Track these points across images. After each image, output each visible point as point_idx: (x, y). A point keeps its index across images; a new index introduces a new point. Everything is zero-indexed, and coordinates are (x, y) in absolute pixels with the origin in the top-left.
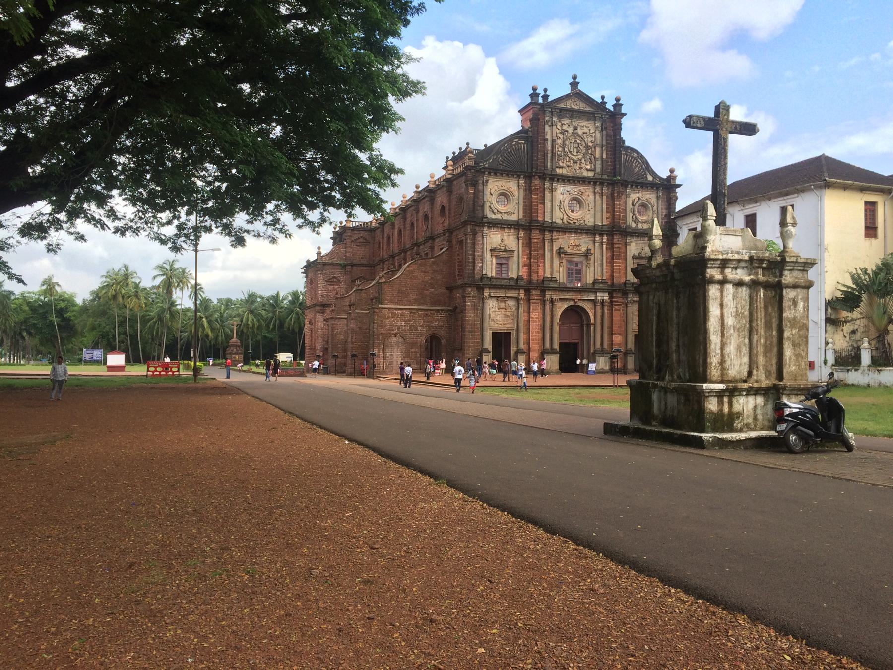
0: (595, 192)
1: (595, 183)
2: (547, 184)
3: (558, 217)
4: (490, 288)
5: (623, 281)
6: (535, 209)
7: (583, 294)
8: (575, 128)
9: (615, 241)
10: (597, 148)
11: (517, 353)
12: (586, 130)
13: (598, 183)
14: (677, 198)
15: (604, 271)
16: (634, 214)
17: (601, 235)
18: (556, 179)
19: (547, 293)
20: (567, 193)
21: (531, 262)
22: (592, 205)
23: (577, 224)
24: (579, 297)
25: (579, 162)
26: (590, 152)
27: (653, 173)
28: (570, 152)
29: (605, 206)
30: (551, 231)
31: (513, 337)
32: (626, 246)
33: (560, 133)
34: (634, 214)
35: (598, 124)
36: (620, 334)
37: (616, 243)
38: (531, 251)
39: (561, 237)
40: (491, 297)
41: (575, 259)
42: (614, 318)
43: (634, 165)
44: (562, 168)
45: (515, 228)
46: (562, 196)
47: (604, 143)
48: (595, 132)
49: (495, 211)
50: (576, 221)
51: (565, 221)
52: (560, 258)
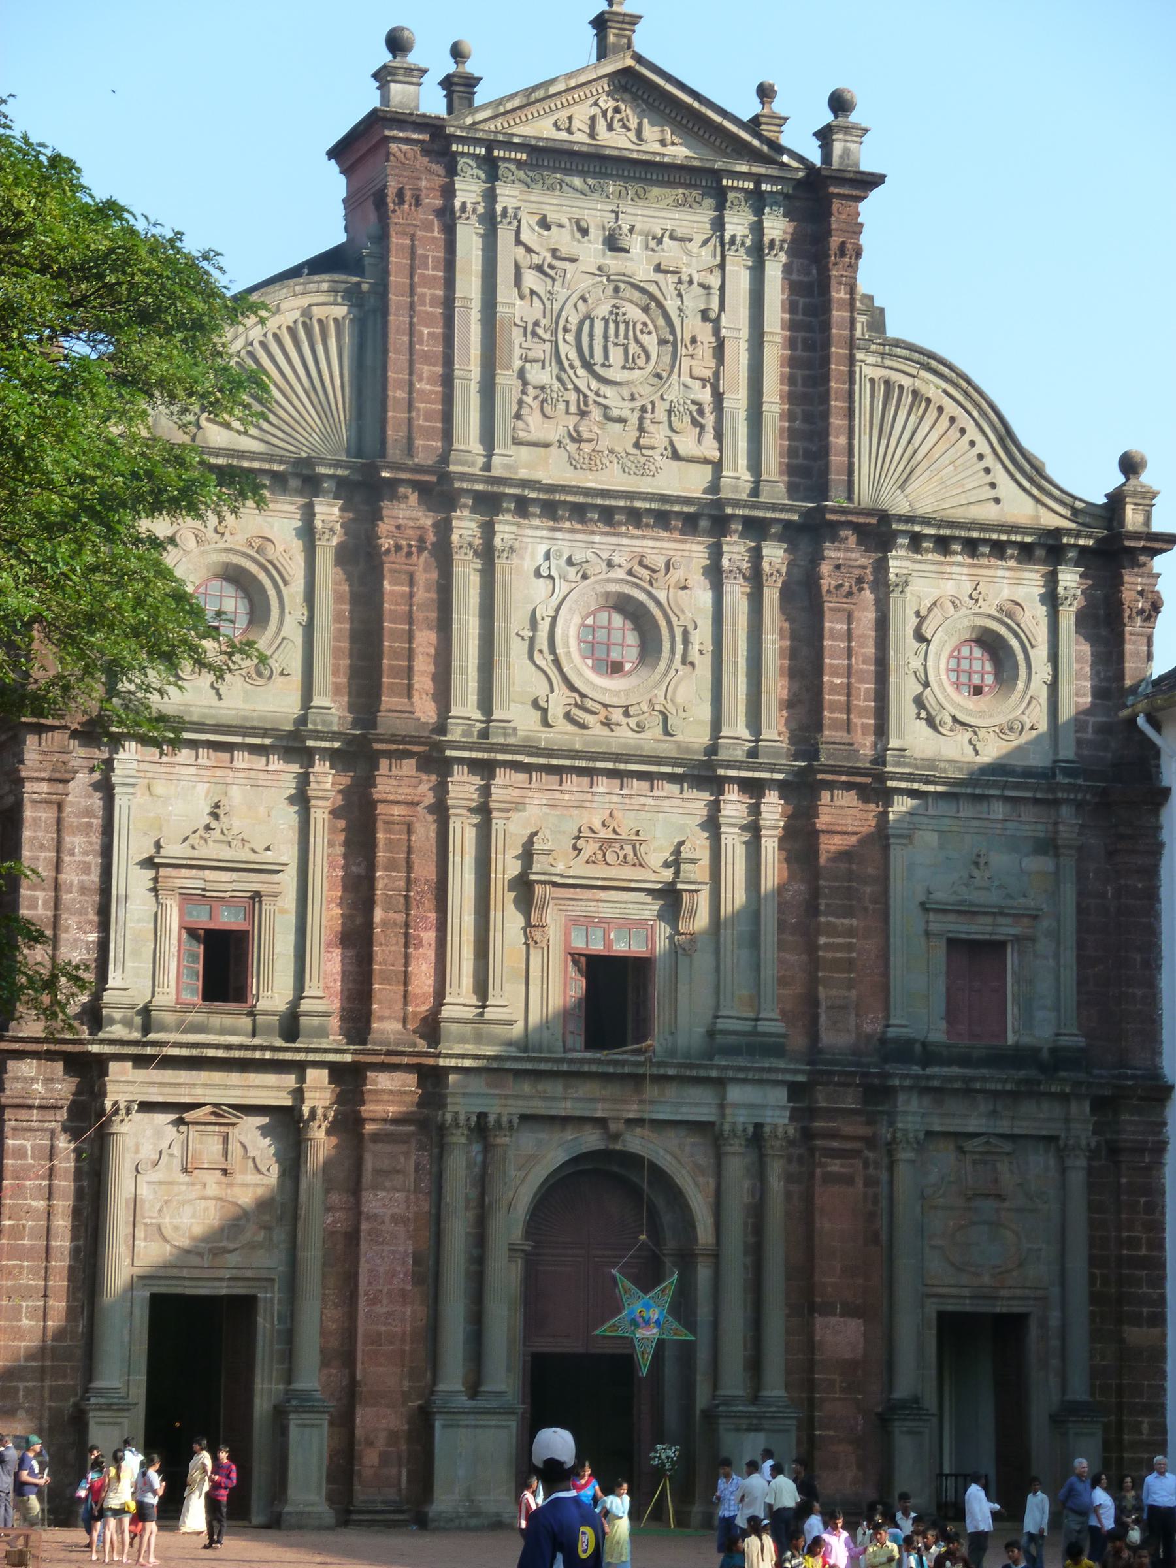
4: (141, 1061)
6: (395, 654)
7: (651, 1091)
9: (824, 819)
11: (280, 1414)
12: (670, 252)
14: (1156, 607)
15: (769, 972)
16: (926, 685)
17: (754, 788)
20: (572, 572)
21: (369, 924)
31: (266, 1324)
33: (539, 268)
35: (738, 224)
36: (850, 1311)
38: (371, 867)
40: (147, 1107)
41: (615, 906)
42: (823, 1224)
44: (547, 445)
46: (542, 585)
48: (722, 266)
50: (617, 715)
51: (556, 712)
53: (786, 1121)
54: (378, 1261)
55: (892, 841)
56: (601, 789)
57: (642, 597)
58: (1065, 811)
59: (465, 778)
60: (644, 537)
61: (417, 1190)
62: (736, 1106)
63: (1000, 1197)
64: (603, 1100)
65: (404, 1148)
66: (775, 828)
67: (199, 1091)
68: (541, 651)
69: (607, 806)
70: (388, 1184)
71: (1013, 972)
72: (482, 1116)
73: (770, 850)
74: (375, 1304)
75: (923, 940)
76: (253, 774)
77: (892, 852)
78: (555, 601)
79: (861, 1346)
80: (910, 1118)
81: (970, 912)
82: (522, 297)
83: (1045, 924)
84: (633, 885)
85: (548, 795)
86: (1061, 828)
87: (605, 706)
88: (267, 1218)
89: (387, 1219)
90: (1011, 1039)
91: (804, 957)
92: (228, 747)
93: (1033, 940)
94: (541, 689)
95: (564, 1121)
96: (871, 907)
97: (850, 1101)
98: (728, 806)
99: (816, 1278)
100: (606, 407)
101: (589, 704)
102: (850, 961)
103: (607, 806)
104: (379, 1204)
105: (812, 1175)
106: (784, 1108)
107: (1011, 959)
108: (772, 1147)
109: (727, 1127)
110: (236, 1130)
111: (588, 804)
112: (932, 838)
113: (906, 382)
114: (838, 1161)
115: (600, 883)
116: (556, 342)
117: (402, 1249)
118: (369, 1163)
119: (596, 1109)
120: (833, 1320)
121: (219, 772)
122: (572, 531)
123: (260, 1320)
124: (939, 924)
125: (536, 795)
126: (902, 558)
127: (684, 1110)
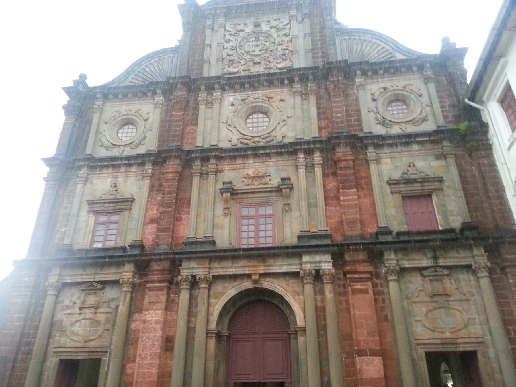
0: (294, 94)
1: (291, 81)
5: (371, 229)
7: (271, 261)
8: (257, 25)
12: (274, 23)
17: (309, 152)
18: (216, 86)
19: (185, 264)
23: (261, 144)
24: (262, 270)
27: (409, 52)
28: (248, 53)
30: (205, 159)
31: (103, 371)
33: (231, 34)
36: (374, 353)
39: (227, 168)
45: (138, 164)
49: (106, 143)
50: (256, 139)
52: (226, 201)
53: (331, 267)
54: (147, 340)
55: (370, 162)
57: (266, 105)
58: (445, 143)
60: (266, 90)
61: (166, 309)
63: (447, 295)
64: (248, 266)
65: (163, 292)
67: (85, 277)
68: (229, 125)
69: (254, 167)
70: (154, 308)
71: (436, 203)
72: (194, 277)
74: (144, 360)
75: (390, 196)
76: (126, 173)
77: (370, 166)
79: (382, 370)
80: (392, 262)
81: (409, 182)
82: (227, 42)
83: (446, 184)
85: (231, 166)
86: (444, 148)
87: (252, 137)
88: (108, 326)
89: (153, 322)
90: (441, 228)
91: (338, 208)
92: (119, 166)
93: (442, 190)
95: (234, 277)
96: (365, 187)
97: (361, 256)
98: (300, 159)
100: (253, 61)
101: (246, 137)
103: (254, 167)
104: (150, 316)
106: (329, 262)
107: (434, 198)
108: (326, 279)
109: (302, 273)
110: (102, 292)
111: (247, 167)
112: (388, 160)
113: (357, 38)
114: (359, 284)
115: (250, 191)
116: (237, 49)
117: (158, 335)
118: (147, 300)
119: (245, 271)
120: (365, 358)
121: (115, 174)
123: (101, 370)
124: (396, 188)
125: (227, 167)
126: (361, 78)
127: (285, 267)
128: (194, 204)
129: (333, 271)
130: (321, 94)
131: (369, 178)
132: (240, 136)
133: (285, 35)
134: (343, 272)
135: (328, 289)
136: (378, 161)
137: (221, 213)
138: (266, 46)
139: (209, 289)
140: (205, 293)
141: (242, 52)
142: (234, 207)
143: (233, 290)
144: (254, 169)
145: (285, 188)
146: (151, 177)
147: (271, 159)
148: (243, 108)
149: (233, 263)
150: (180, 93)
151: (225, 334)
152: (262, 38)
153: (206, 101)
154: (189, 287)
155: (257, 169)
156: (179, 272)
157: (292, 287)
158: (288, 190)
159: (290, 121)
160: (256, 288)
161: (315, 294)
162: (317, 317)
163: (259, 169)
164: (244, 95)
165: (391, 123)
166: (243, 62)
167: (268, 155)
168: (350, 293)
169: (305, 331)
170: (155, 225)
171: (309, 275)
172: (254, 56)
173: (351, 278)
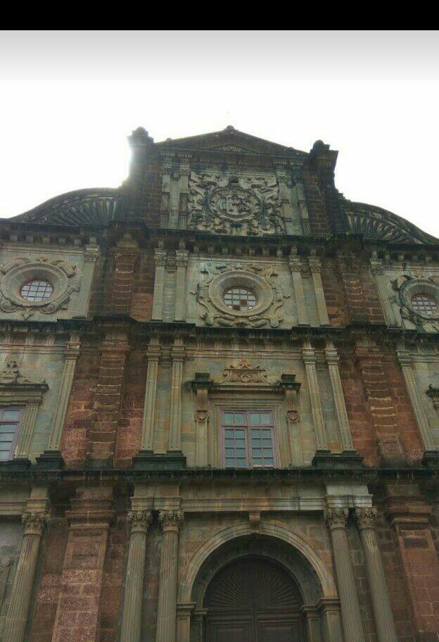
1: (287, 253)
2: (160, 254)
3: (194, 314)
5: (415, 456)
7: (279, 495)
8: (234, 181)
10: (284, 205)
12: (257, 182)
13: (294, 250)
17: (319, 344)
18: (182, 244)
19: (139, 493)
22: (284, 290)
24: (265, 506)
25: (245, 226)
26: (270, 211)
29: (319, 291)
30: (167, 340)
32: (401, 369)
33: (199, 186)
34: (403, 305)
35: (280, 173)
37: (367, 358)
39: (201, 354)
43: (379, 229)
46: (202, 275)
47: (301, 198)
50: (241, 320)
51: (211, 320)
52: (201, 401)
53: (371, 506)
56: (237, 349)
59: (157, 343)
62: (333, 497)
66: (334, 361)
73: (334, 371)
75: (434, 411)
78: (209, 280)
84: (257, 389)
87: (236, 317)
94: (202, 312)
99: (416, 613)
101: (227, 315)
102: (392, 420)
105: (397, 544)
106: (366, 497)
108: (365, 522)
112: (425, 365)
114: (412, 532)
115: (238, 389)
119: (239, 507)
122: (216, 257)
126: (377, 261)
128: (150, 400)
129: (375, 511)
130: (328, 273)
131: (402, 384)
132: (218, 314)
133: (271, 198)
134: (384, 514)
135: (370, 539)
136: (412, 364)
137: (193, 418)
138: (248, 207)
139: (179, 536)
140: (174, 541)
141: (215, 209)
142: (213, 411)
143: (217, 536)
144: (241, 360)
145: (289, 389)
146: (78, 357)
147: (264, 348)
148: (220, 278)
149: (218, 494)
150: (128, 245)
151: (202, 613)
152: (243, 198)
153: (166, 261)
154: (145, 530)
155: (245, 359)
156: (130, 506)
157: (311, 536)
158: (295, 392)
159: (289, 303)
160: (254, 535)
161: (350, 549)
162: (356, 581)
163: (248, 360)
164: (221, 262)
165: (422, 320)
166: (217, 221)
167: (260, 343)
168: (402, 545)
169: (339, 605)
170: (83, 430)
171: (339, 517)
172: (234, 216)
173: (401, 523)
